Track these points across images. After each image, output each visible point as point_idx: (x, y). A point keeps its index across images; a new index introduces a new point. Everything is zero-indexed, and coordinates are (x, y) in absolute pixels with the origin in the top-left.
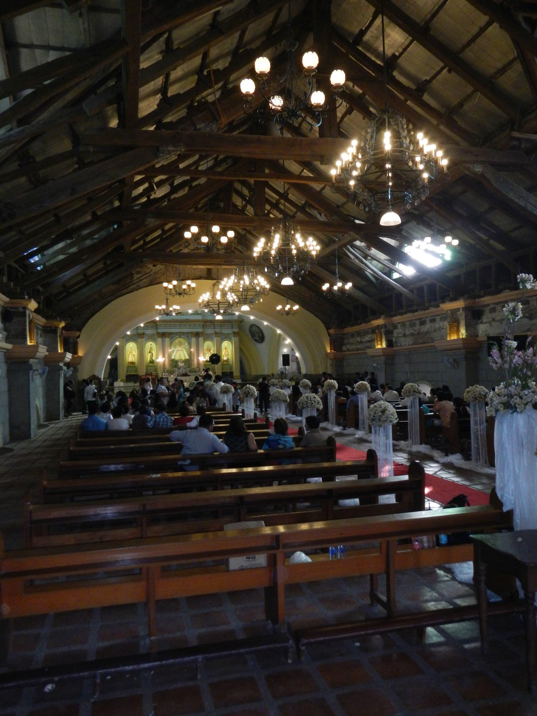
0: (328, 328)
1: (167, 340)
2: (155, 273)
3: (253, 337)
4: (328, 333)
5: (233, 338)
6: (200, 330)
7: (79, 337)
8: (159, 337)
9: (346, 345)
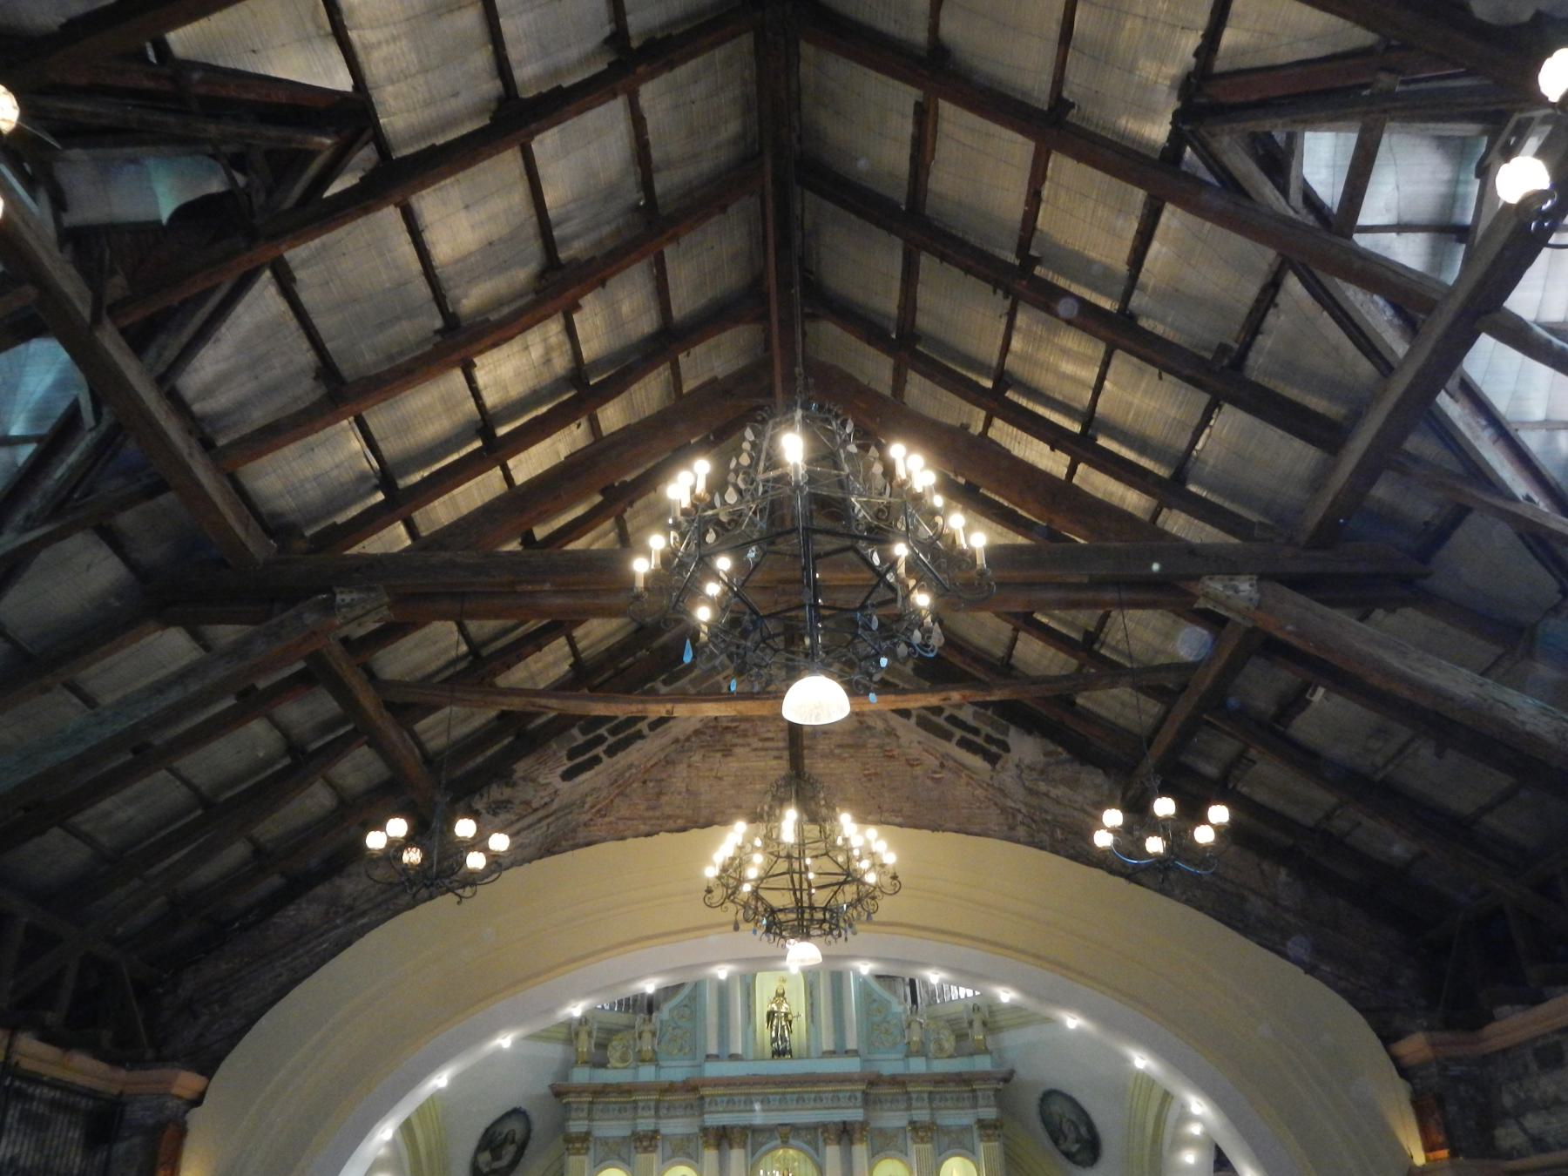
0: (1388, 1038)
1: (737, 1156)
2: (567, 808)
3: (1056, 1142)
4: (1396, 1060)
5: (981, 1147)
6: (855, 1115)
7: (197, 1101)
8: (707, 1145)
9: (1518, 1114)
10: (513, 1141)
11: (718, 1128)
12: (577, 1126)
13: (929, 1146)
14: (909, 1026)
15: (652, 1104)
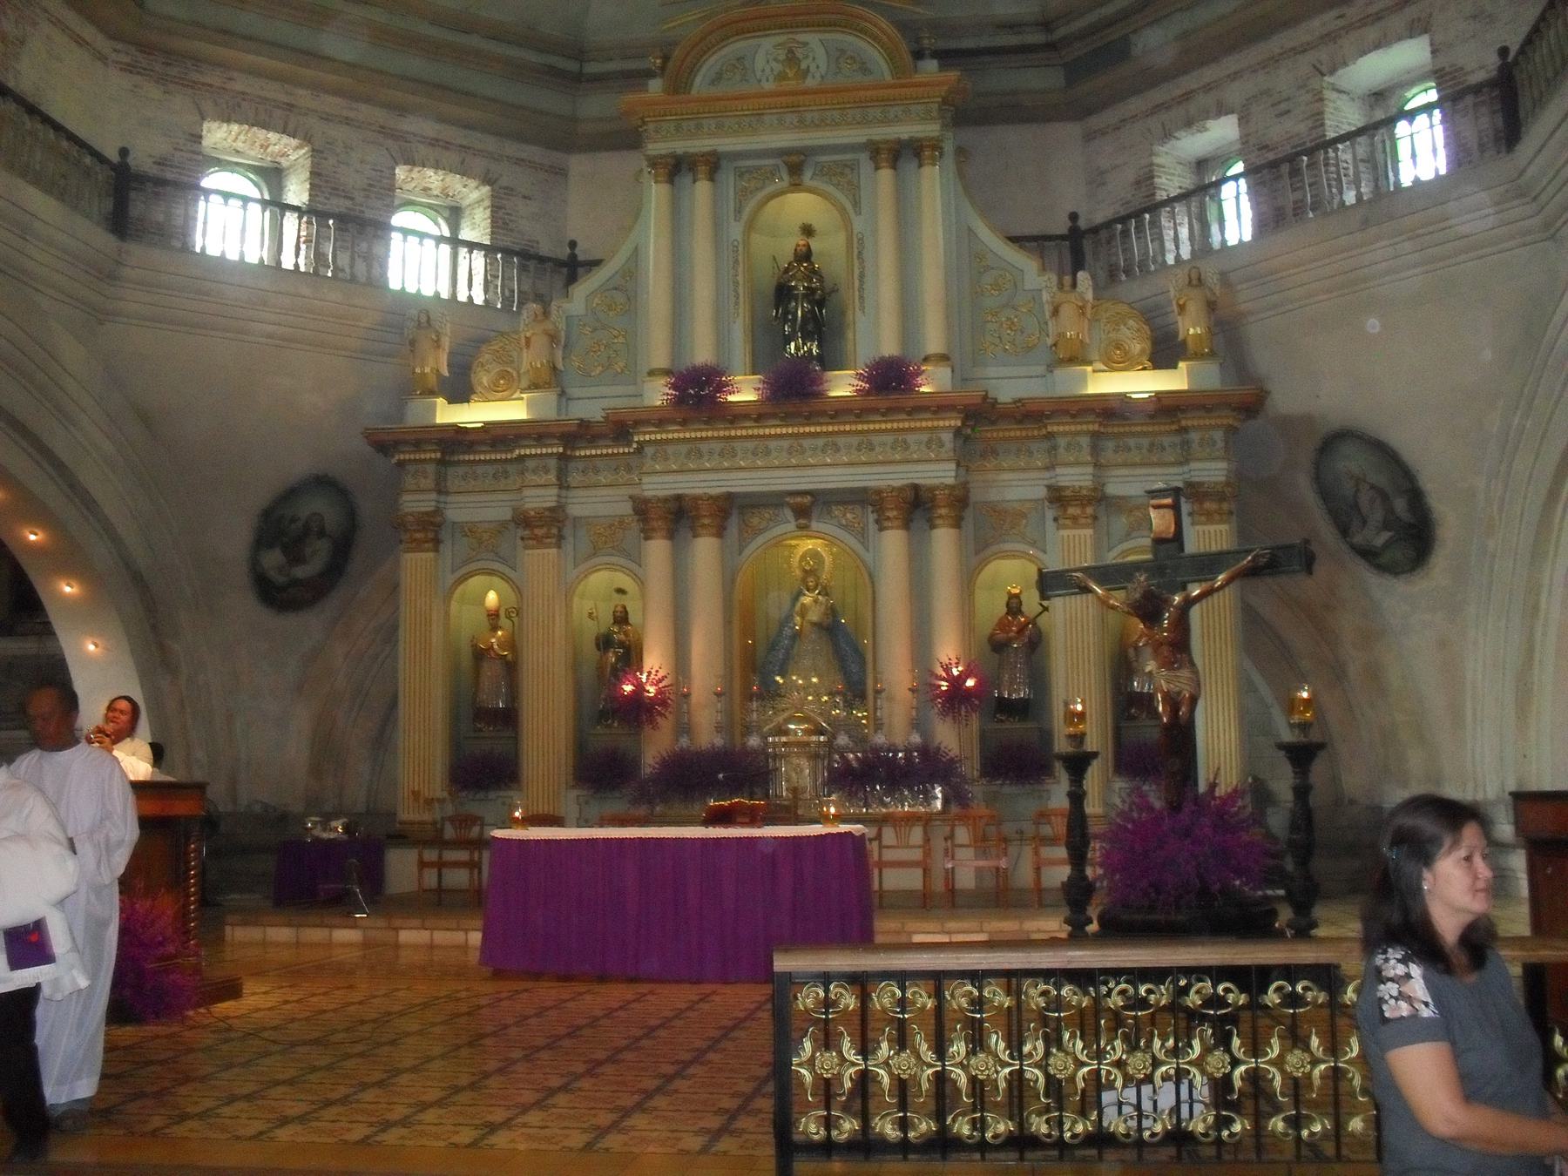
3: (1344, 531)
6: (939, 473)
10: (322, 533)
11: (666, 500)
12: (416, 503)
13: (1089, 532)
14: (1056, 312)
15: (553, 463)
